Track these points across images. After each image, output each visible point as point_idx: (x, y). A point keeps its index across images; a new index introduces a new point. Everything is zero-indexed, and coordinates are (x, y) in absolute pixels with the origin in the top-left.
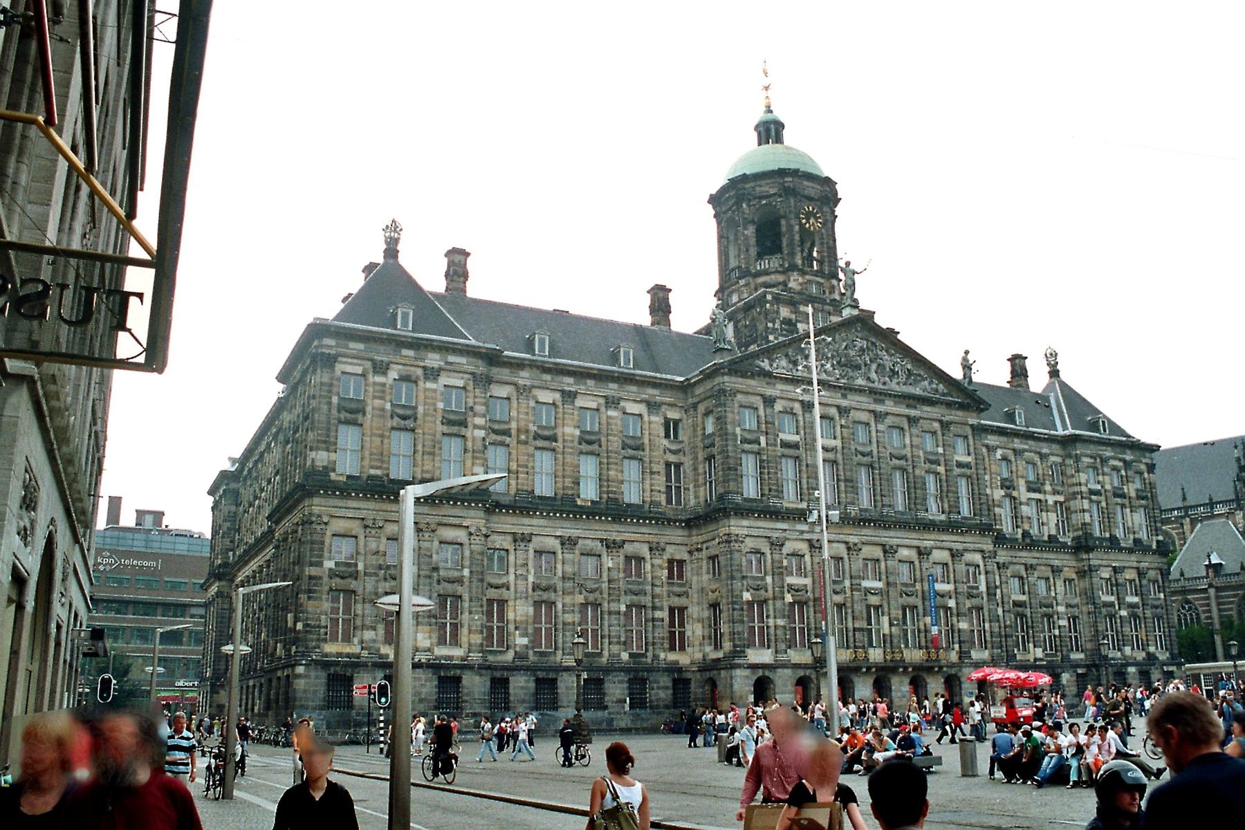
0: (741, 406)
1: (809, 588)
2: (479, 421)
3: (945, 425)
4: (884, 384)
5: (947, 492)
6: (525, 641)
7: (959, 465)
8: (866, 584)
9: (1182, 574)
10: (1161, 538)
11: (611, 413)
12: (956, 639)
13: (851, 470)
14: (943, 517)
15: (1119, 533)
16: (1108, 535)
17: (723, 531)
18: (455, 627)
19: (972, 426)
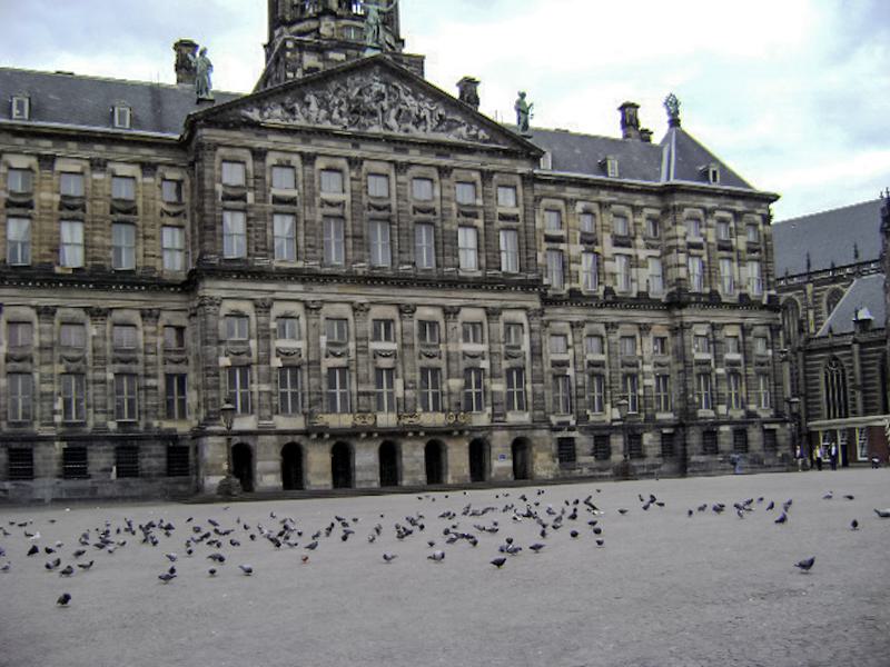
0: (224, 161)
1: (303, 353)
3: (487, 176)
4: (407, 131)
5: (487, 246)
7: (503, 217)
8: (374, 346)
9: (831, 331)
10: (773, 292)
11: (98, 176)
12: (489, 402)
13: (361, 226)
14: (479, 274)
15: (724, 290)
16: (707, 290)
17: (201, 293)
19: (521, 175)
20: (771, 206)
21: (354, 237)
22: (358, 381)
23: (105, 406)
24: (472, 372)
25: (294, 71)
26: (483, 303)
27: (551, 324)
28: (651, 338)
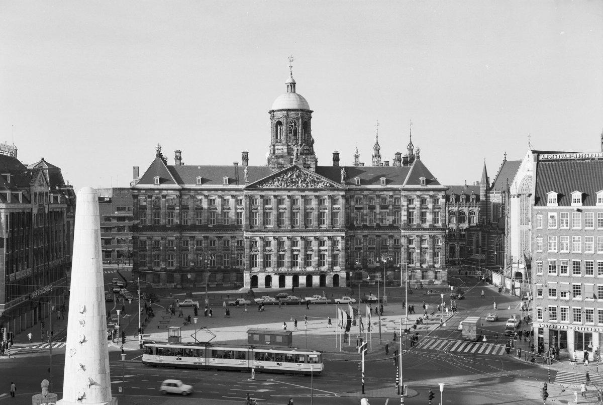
2: (178, 208)
3: (330, 197)
6: (193, 264)
16: (416, 223)
18: (172, 262)
19: (342, 196)
24: (321, 257)
25: (274, 165)
26: (326, 235)
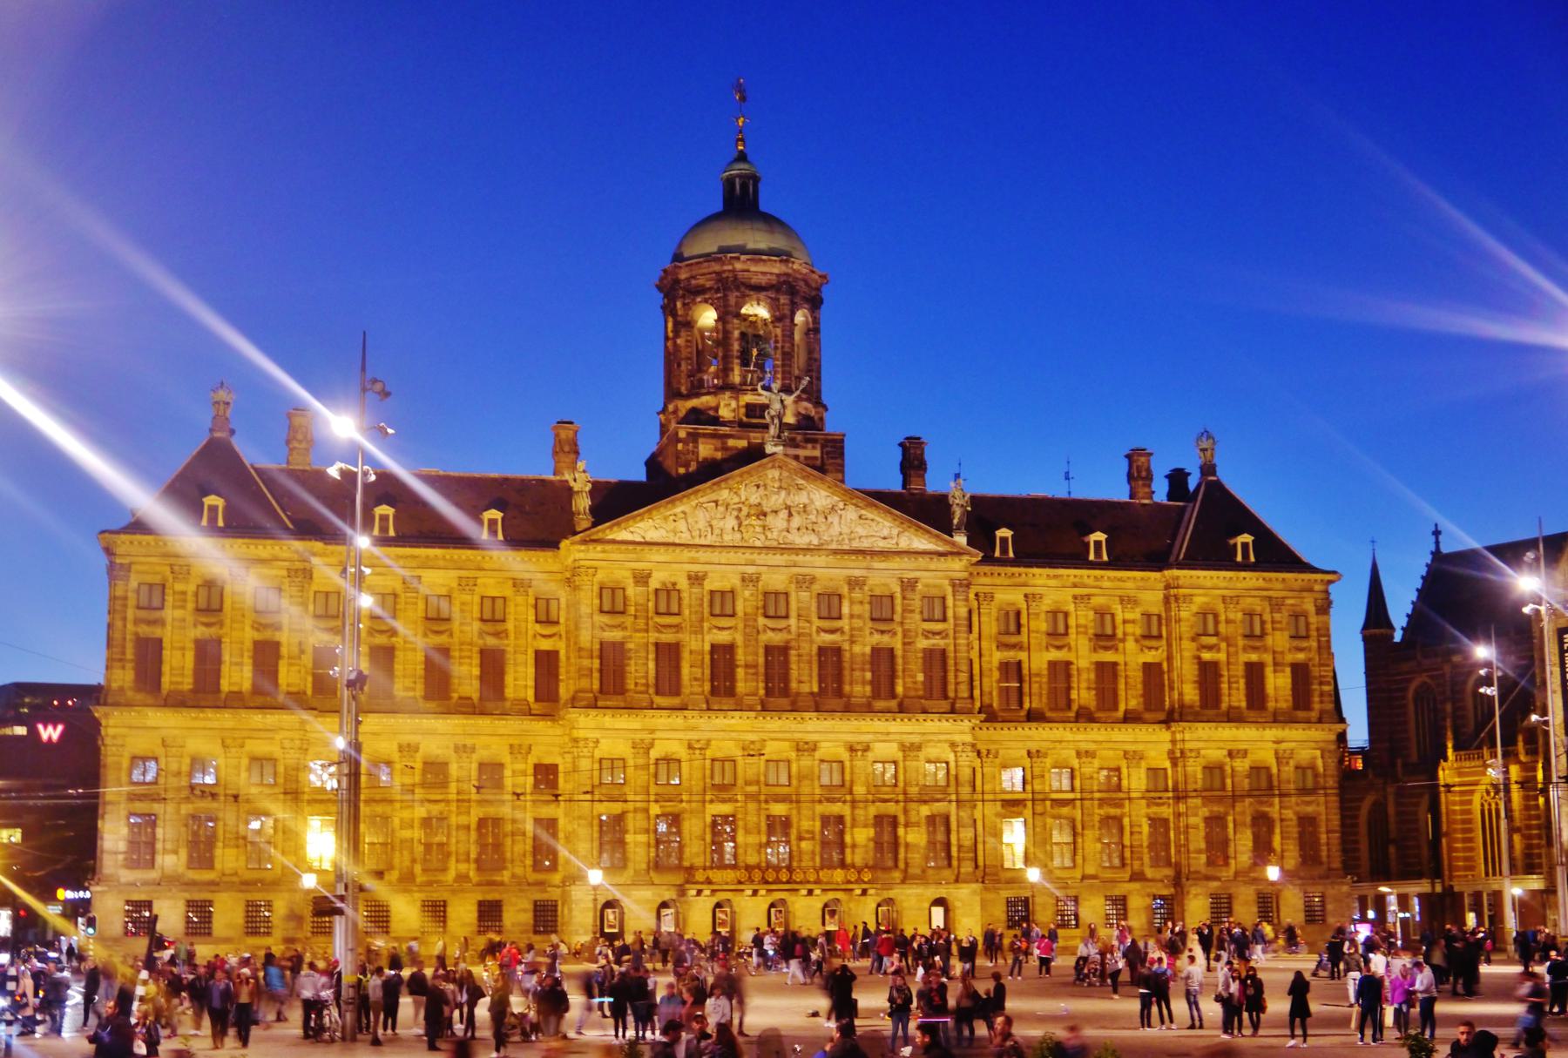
13: (756, 654)
20: (1331, 588)
21: (747, 666)
22: (747, 832)
23: (468, 854)
25: (687, 465)
26: (897, 737)
27: (1001, 752)
28: (1143, 773)
